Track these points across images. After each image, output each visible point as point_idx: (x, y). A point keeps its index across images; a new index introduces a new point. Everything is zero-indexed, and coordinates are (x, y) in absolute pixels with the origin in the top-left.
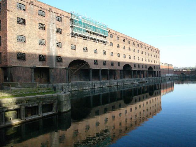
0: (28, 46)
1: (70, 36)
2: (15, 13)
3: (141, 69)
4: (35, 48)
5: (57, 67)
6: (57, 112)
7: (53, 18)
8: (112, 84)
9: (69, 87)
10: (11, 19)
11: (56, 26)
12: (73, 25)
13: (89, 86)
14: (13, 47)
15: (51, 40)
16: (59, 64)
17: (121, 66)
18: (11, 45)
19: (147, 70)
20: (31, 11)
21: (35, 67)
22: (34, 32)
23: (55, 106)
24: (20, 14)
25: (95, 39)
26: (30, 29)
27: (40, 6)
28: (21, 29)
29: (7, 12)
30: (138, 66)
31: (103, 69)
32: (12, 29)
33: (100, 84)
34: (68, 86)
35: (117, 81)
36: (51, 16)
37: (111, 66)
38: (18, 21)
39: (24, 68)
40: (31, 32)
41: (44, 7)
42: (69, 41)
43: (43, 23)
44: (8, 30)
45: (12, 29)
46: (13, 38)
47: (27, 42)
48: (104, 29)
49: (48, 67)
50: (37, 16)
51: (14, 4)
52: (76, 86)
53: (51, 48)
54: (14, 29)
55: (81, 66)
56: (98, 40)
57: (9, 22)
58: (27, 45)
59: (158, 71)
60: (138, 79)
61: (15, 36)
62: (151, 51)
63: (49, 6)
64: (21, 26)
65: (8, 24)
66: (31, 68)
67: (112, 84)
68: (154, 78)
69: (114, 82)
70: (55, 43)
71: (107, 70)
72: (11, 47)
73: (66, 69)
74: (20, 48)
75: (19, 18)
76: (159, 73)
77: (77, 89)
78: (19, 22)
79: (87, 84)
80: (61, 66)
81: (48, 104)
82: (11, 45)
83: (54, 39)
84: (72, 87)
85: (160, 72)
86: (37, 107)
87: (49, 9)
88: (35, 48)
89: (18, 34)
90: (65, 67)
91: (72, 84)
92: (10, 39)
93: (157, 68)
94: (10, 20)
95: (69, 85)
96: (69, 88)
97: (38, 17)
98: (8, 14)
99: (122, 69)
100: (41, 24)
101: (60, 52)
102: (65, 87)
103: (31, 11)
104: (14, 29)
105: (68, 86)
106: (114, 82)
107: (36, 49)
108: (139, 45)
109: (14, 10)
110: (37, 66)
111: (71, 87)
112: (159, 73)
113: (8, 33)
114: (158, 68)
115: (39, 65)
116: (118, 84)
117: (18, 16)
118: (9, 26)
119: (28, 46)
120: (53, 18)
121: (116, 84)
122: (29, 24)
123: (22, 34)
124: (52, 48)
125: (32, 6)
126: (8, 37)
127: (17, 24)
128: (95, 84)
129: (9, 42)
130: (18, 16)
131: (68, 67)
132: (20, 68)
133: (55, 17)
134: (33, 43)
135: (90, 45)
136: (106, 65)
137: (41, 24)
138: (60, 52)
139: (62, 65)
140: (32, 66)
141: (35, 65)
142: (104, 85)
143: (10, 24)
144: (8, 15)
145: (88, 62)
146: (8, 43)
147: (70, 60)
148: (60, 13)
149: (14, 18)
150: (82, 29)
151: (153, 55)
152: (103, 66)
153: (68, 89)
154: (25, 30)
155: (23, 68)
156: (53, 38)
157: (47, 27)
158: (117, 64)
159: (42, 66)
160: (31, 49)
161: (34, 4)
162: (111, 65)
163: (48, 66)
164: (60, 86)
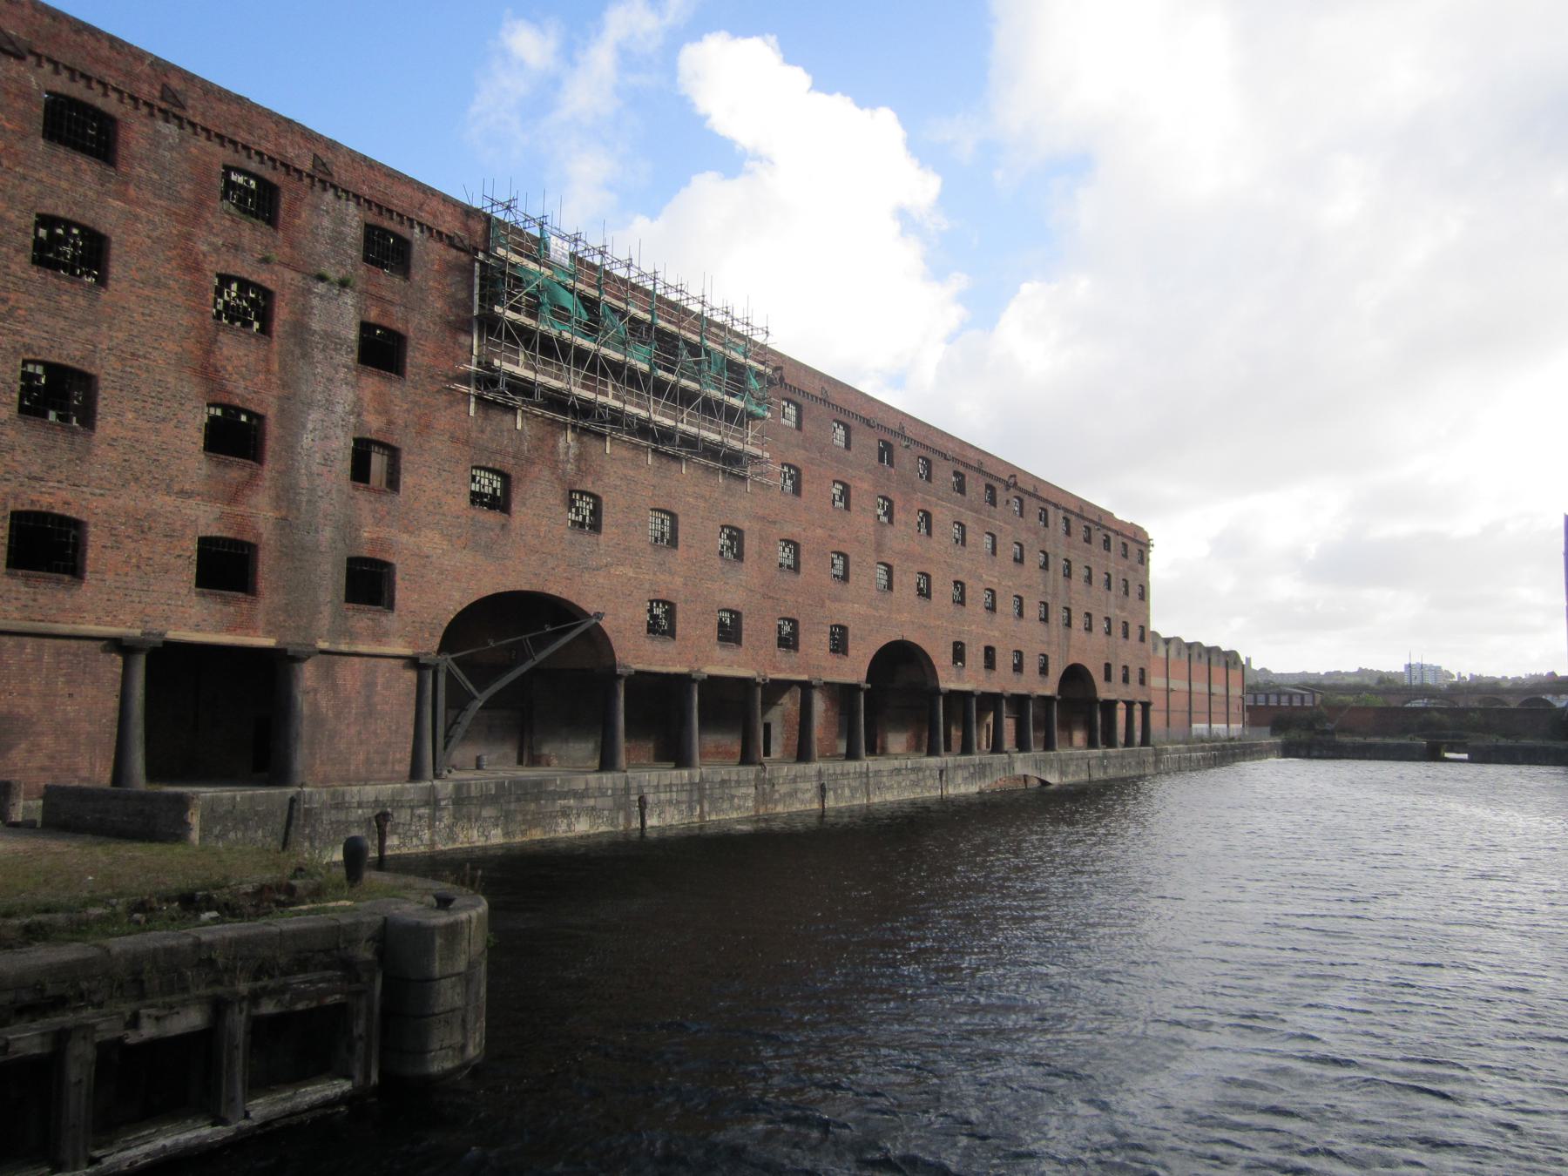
1: (469, 394)
2: (24, 178)
3: (1002, 682)
5: (343, 648)
6: (374, 1078)
7: (337, 238)
8: (783, 797)
9: (433, 818)
11: (359, 310)
12: (498, 309)
13: (593, 812)
15: (314, 417)
16: (362, 619)
17: (852, 652)
19: (1050, 687)
22: (171, 346)
23: (359, 1028)
24: (64, 184)
25: (666, 435)
30: (982, 659)
31: (711, 677)
33: (684, 796)
34: (422, 811)
35: (820, 774)
36: (326, 222)
37: (780, 653)
38: (39, 245)
39: (59, 642)
42: (458, 433)
43: (254, 278)
47: (106, 424)
48: (741, 359)
49: (269, 642)
52: (487, 812)
53: (304, 482)
55: (540, 644)
56: (690, 442)
59: (1130, 705)
60: (976, 758)
62: (1088, 540)
66: (118, 645)
67: (783, 797)
68: (1098, 752)
69: (794, 780)
70: (342, 446)
71: (746, 684)
73: (414, 662)
74: (36, 469)
75: (46, 221)
76: (1138, 714)
77: (496, 837)
78: (45, 255)
79: (580, 795)
80: (379, 636)
81: (300, 1007)
83: (339, 409)
84: (457, 818)
85: (1146, 706)
86: (203, 1043)
89: (28, 348)
90: (408, 652)
91: (459, 788)
93: (1126, 679)
95: (432, 801)
96: (431, 826)
99: (864, 676)
101: (378, 522)
102: (403, 816)
105: (426, 804)
106: (794, 780)
107: (176, 488)
108: (1001, 494)
109: (21, 146)
110: (174, 635)
111: (447, 820)
112: (1138, 714)
114: (1134, 677)
115: (197, 628)
116: (823, 797)
117: (48, 202)
120: (337, 238)
121: (808, 796)
123: (69, 354)
124: (312, 490)
127: (35, 274)
128: (650, 798)
130: (48, 202)
131: (440, 651)
132: (29, 642)
133: (353, 230)
134: (157, 431)
135: (624, 478)
136: (738, 641)
137: (234, 286)
138: (378, 522)
139: (386, 634)
140: (137, 632)
141: (156, 626)
142: (715, 809)
145: (599, 616)
147: (457, 595)
148: (397, 204)
149: (12, 215)
150: (565, 346)
151: (1099, 578)
152: (719, 652)
153: (426, 835)
155: (48, 642)
156: (329, 405)
157: (282, 314)
158: (826, 638)
159: (218, 632)
161: (189, 114)
162: (776, 642)
163: (269, 634)
164: (360, 805)
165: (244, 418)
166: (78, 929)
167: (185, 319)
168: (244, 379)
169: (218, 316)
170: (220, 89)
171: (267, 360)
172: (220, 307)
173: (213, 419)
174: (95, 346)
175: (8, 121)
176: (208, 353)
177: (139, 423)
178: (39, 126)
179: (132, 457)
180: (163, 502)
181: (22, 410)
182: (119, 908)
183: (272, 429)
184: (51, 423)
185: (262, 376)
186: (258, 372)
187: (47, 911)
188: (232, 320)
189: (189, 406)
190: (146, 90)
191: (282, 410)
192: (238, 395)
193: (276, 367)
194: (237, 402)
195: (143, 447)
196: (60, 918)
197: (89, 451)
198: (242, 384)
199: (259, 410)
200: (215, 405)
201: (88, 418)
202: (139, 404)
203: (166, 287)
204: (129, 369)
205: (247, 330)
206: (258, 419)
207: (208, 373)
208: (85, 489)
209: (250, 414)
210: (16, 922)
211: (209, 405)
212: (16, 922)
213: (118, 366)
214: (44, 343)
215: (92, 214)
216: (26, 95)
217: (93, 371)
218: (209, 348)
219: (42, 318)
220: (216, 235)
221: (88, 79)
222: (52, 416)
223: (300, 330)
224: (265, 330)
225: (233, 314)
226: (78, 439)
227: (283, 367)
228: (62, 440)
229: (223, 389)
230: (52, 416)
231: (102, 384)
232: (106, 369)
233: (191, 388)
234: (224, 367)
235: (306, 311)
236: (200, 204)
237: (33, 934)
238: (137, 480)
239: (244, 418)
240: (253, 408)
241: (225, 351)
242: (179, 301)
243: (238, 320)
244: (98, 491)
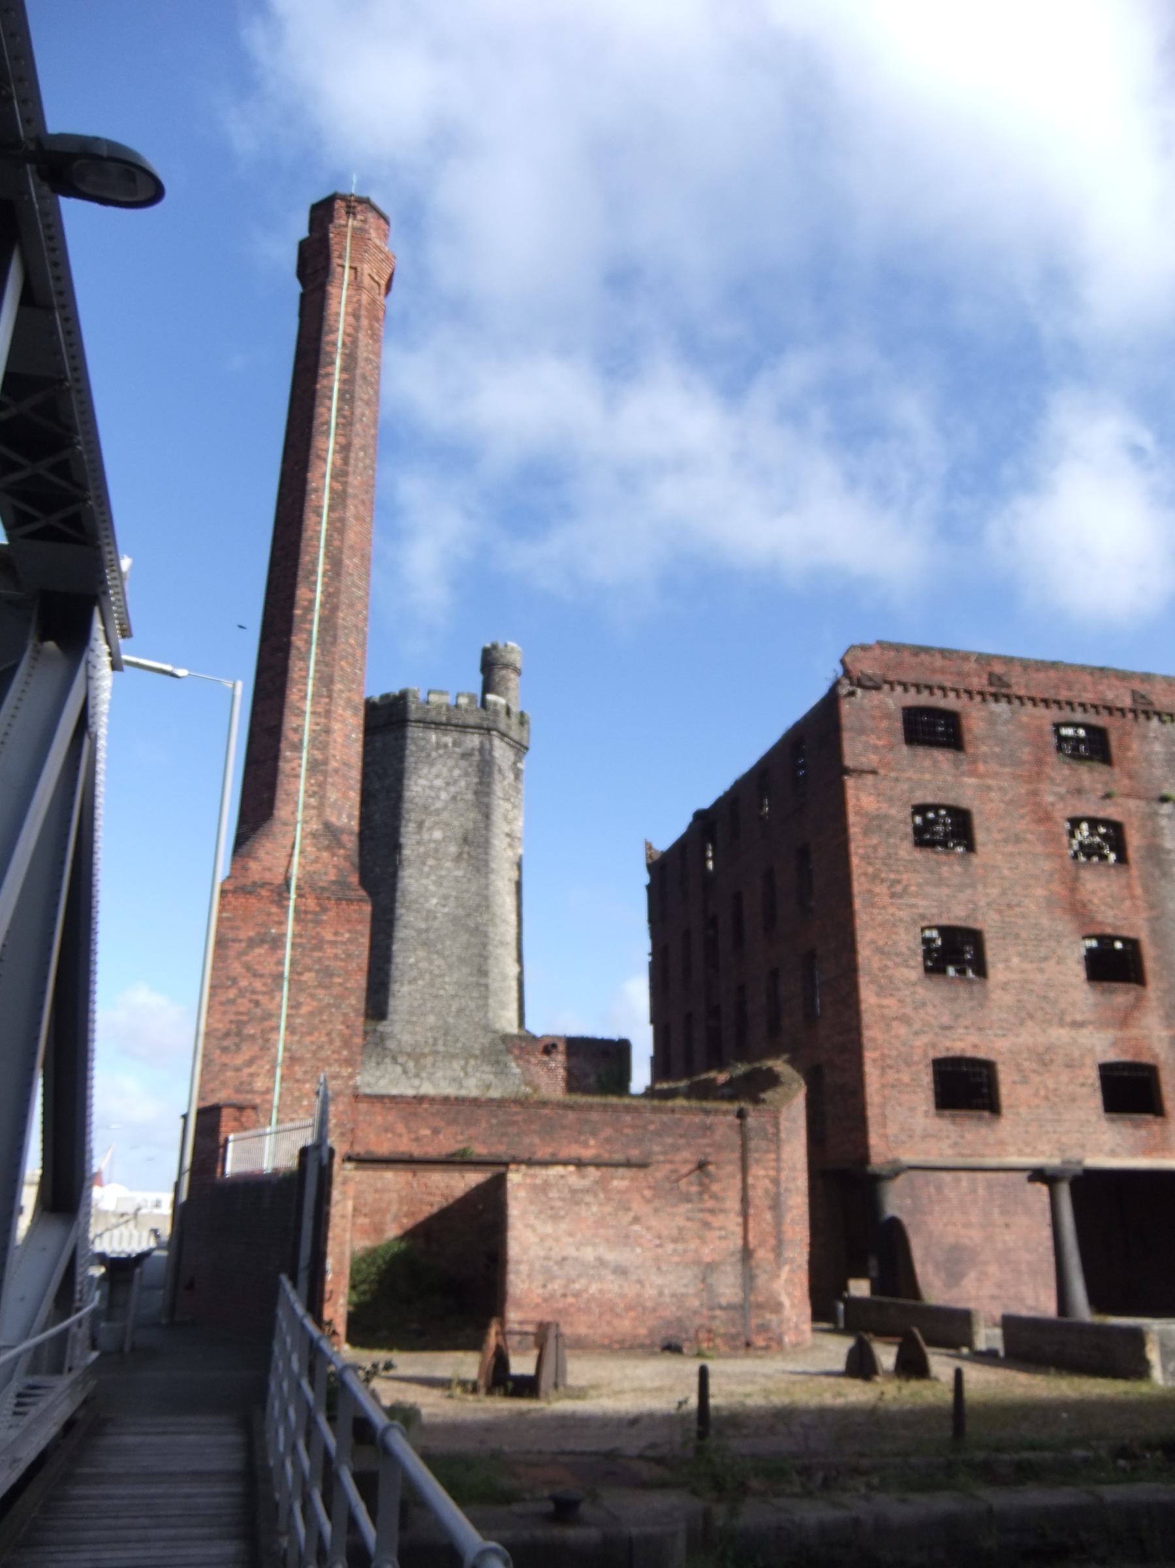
0: (1008, 999)
2: (897, 780)
4: (1063, 1012)
10: (875, 823)
14: (905, 1020)
18: (885, 1002)
20: (1001, 742)
21: (1078, 1170)
22: (1040, 892)
24: (928, 777)
26: (1006, 872)
27: (1064, 695)
28: (941, 882)
29: (850, 782)
32: (881, 889)
38: (918, 831)
40: (1018, 889)
41: (1088, 697)
43: (1101, 814)
44: (858, 903)
45: (881, 889)
46: (897, 955)
47: (997, 972)
50: (1047, 770)
51: (884, 724)
54: (898, 888)
57: (859, 846)
58: (996, 995)
61: (909, 942)
63: (1123, 676)
64: (943, 858)
65: (855, 861)
72: (883, 1017)
74: (946, 1019)
75: (920, 809)
78: (924, 838)
82: (885, 1002)
87: (1127, 702)
88: (1063, 1012)
92: (876, 963)
94: (866, 832)
97: (1058, 779)
98: (850, 793)
100: (1084, 826)
103: (1001, 742)
104: (898, 888)
109: (890, 756)
113: (862, 917)
118: (865, 874)
119: (1008, 999)
122: (998, 836)
123: (956, 916)
125: (1002, 708)
126: (865, 953)
127: (919, 855)
129: (874, 987)
134: (1042, 971)
137: (1084, 826)
143: (865, 858)
144: (851, 803)
146: (868, 996)
149: (893, 811)
154: (973, 886)
157: (1134, 841)
160: (1029, 1023)
165: (1118, 945)
166: (1066, 1472)
167: (1047, 865)
168: (1111, 908)
169: (1075, 856)
170: (1037, 662)
171: (1129, 886)
172: (1076, 847)
173: (1090, 951)
174: (975, 904)
175: (879, 738)
176: (1073, 890)
177: (1027, 966)
178: (900, 736)
179: (1025, 997)
180: (1060, 1035)
181: (928, 970)
182: (1103, 1453)
183: (1149, 953)
184: (952, 978)
185: (1128, 903)
186: (1123, 900)
187: (1033, 1448)
188: (1089, 856)
189: (1065, 942)
190: (978, 682)
191: (1154, 932)
192: (1109, 925)
193: (1139, 891)
194: (1109, 931)
195: (1031, 987)
196: (1048, 1455)
197: (986, 997)
198: (1110, 913)
199: (1131, 934)
200: (1090, 937)
201: (981, 970)
202: (1021, 948)
203: (1025, 840)
204: (1007, 919)
205: (1104, 863)
206: (1133, 945)
207: (1078, 910)
208: (990, 1032)
209: (1124, 940)
210: (1006, 1457)
211: (1085, 938)
212: (1006, 1457)
213: (996, 917)
214: (934, 911)
215: (952, 795)
216: (888, 716)
217: (976, 926)
218: (1073, 885)
219: (929, 889)
220: (1059, 785)
221: (930, 688)
222: (951, 971)
223: (1155, 852)
224: (1122, 859)
225: (1088, 850)
226: (976, 988)
227: (1146, 890)
228: (962, 991)
229: (1092, 920)
230: (951, 971)
231: (988, 936)
232: (988, 923)
233: (1065, 925)
234: (1090, 901)
235: (1156, 833)
236: (1040, 762)
237: (1026, 1473)
238: (1031, 1017)
239: (1118, 945)
240: (1125, 933)
241: (1089, 886)
242: (1039, 849)
243: (1094, 854)
244: (1000, 1032)
